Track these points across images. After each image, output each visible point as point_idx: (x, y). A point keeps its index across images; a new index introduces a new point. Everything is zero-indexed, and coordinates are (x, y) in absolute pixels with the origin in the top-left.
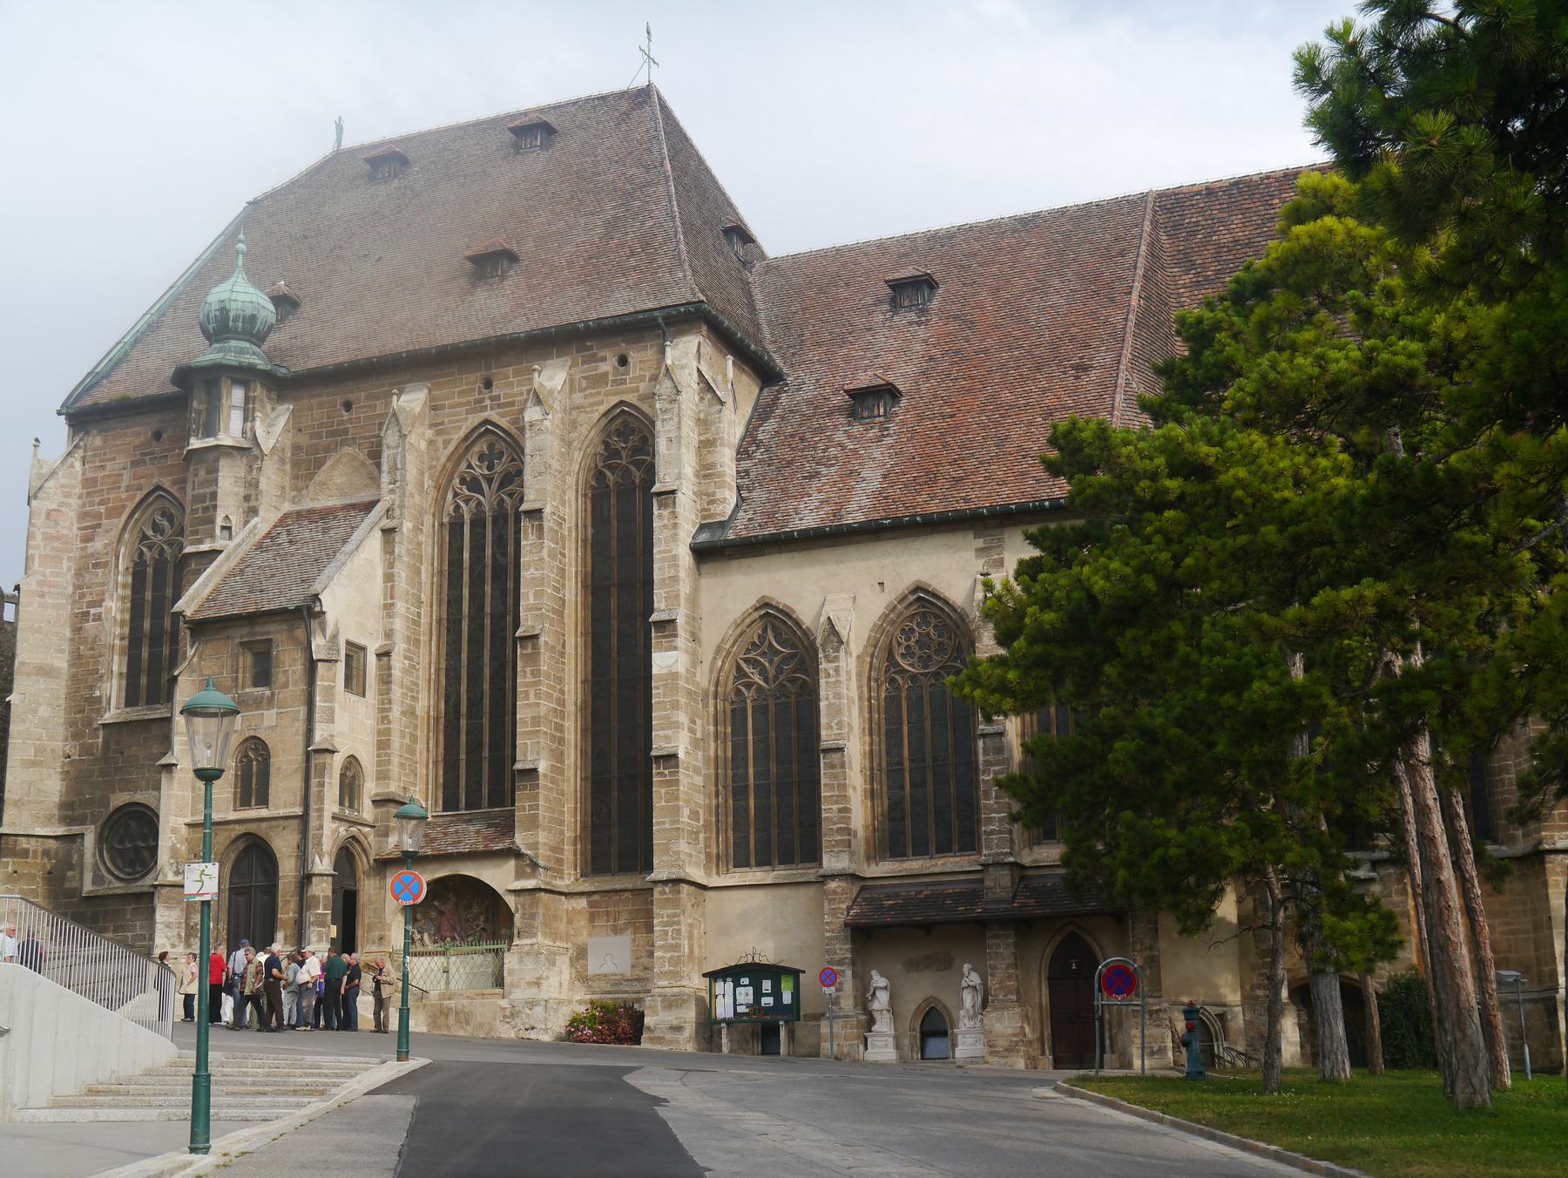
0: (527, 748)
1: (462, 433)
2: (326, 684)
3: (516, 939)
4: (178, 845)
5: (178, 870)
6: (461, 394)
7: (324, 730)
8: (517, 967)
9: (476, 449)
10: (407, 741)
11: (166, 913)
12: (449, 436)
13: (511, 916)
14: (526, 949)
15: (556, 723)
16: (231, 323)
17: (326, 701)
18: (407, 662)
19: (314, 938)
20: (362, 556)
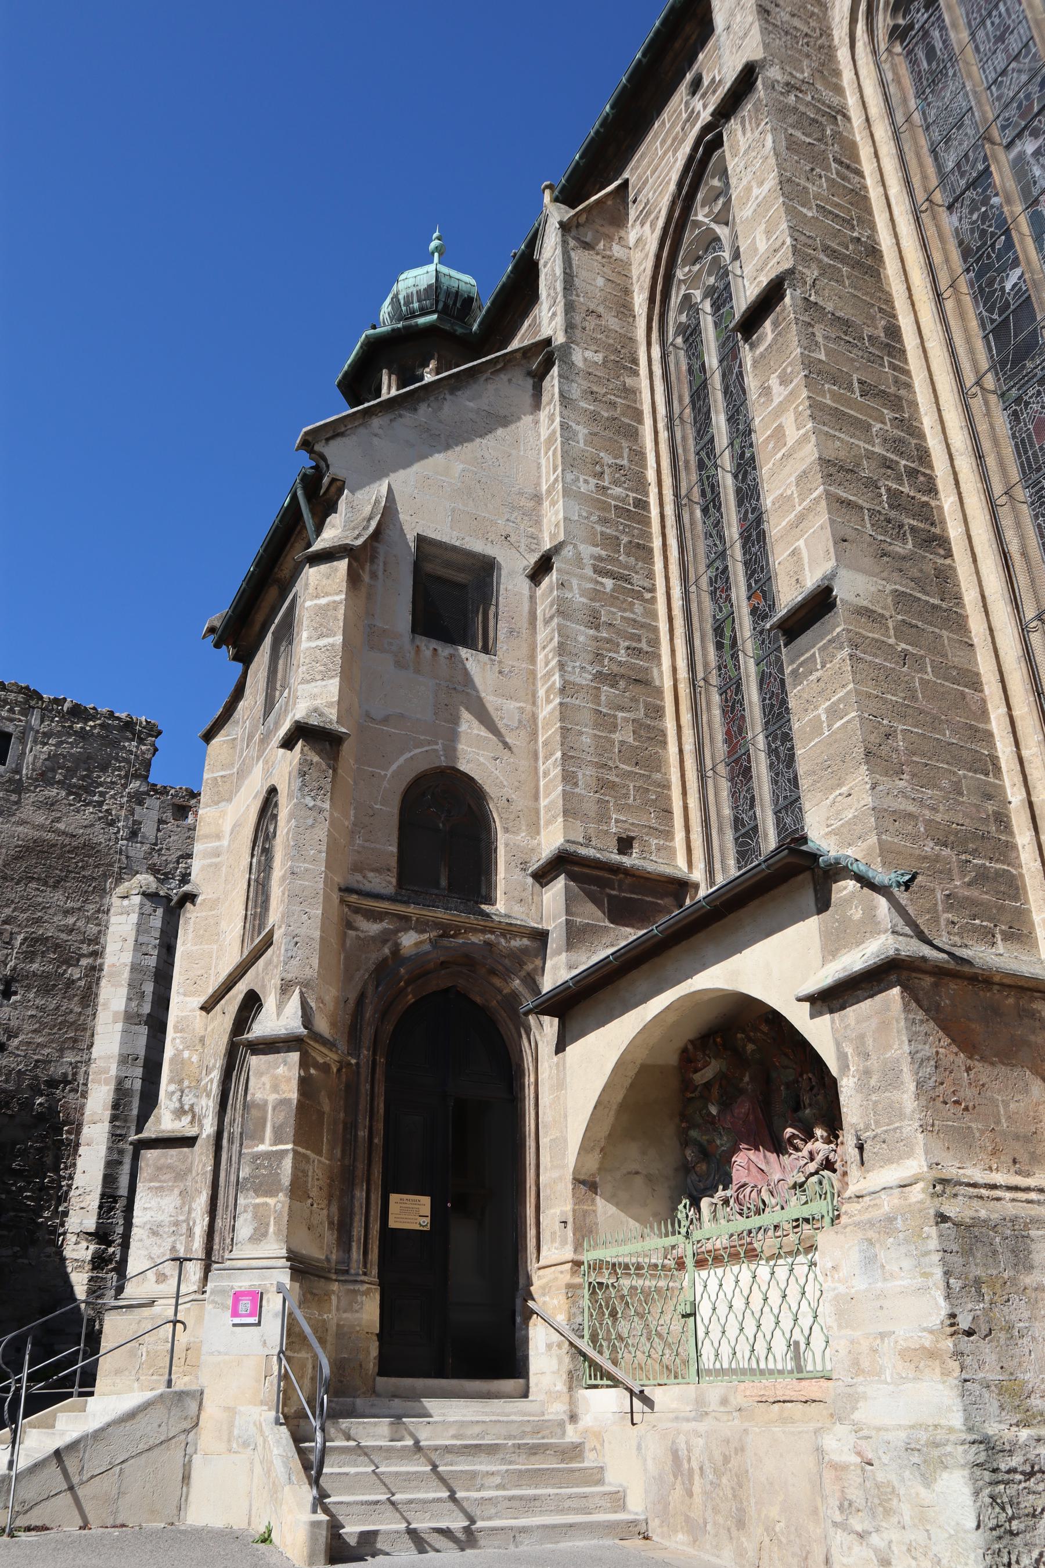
0: (800, 559)
1: (672, 187)
2: (323, 601)
3: (854, 1171)
4: (186, 1054)
5: (182, 1107)
6: (663, 142)
7: (314, 697)
8: (860, 1284)
9: (700, 196)
10: (625, 735)
11: (153, 1203)
12: (657, 209)
13: (834, 1082)
14: (888, 1203)
15: (893, 494)
16: (404, 308)
17: (321, 636)
18: (609, 583)
19: (244, 1228)
20: (471, 404)
